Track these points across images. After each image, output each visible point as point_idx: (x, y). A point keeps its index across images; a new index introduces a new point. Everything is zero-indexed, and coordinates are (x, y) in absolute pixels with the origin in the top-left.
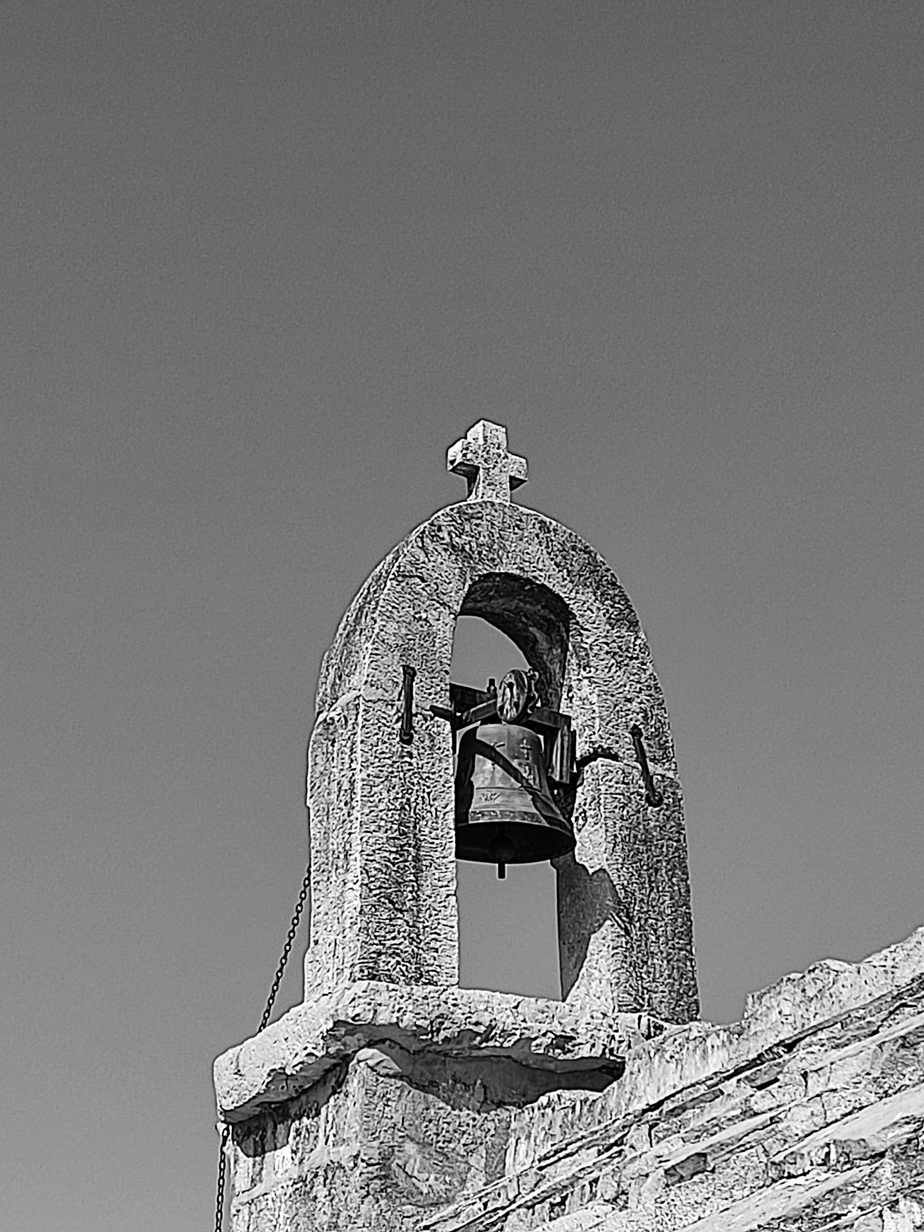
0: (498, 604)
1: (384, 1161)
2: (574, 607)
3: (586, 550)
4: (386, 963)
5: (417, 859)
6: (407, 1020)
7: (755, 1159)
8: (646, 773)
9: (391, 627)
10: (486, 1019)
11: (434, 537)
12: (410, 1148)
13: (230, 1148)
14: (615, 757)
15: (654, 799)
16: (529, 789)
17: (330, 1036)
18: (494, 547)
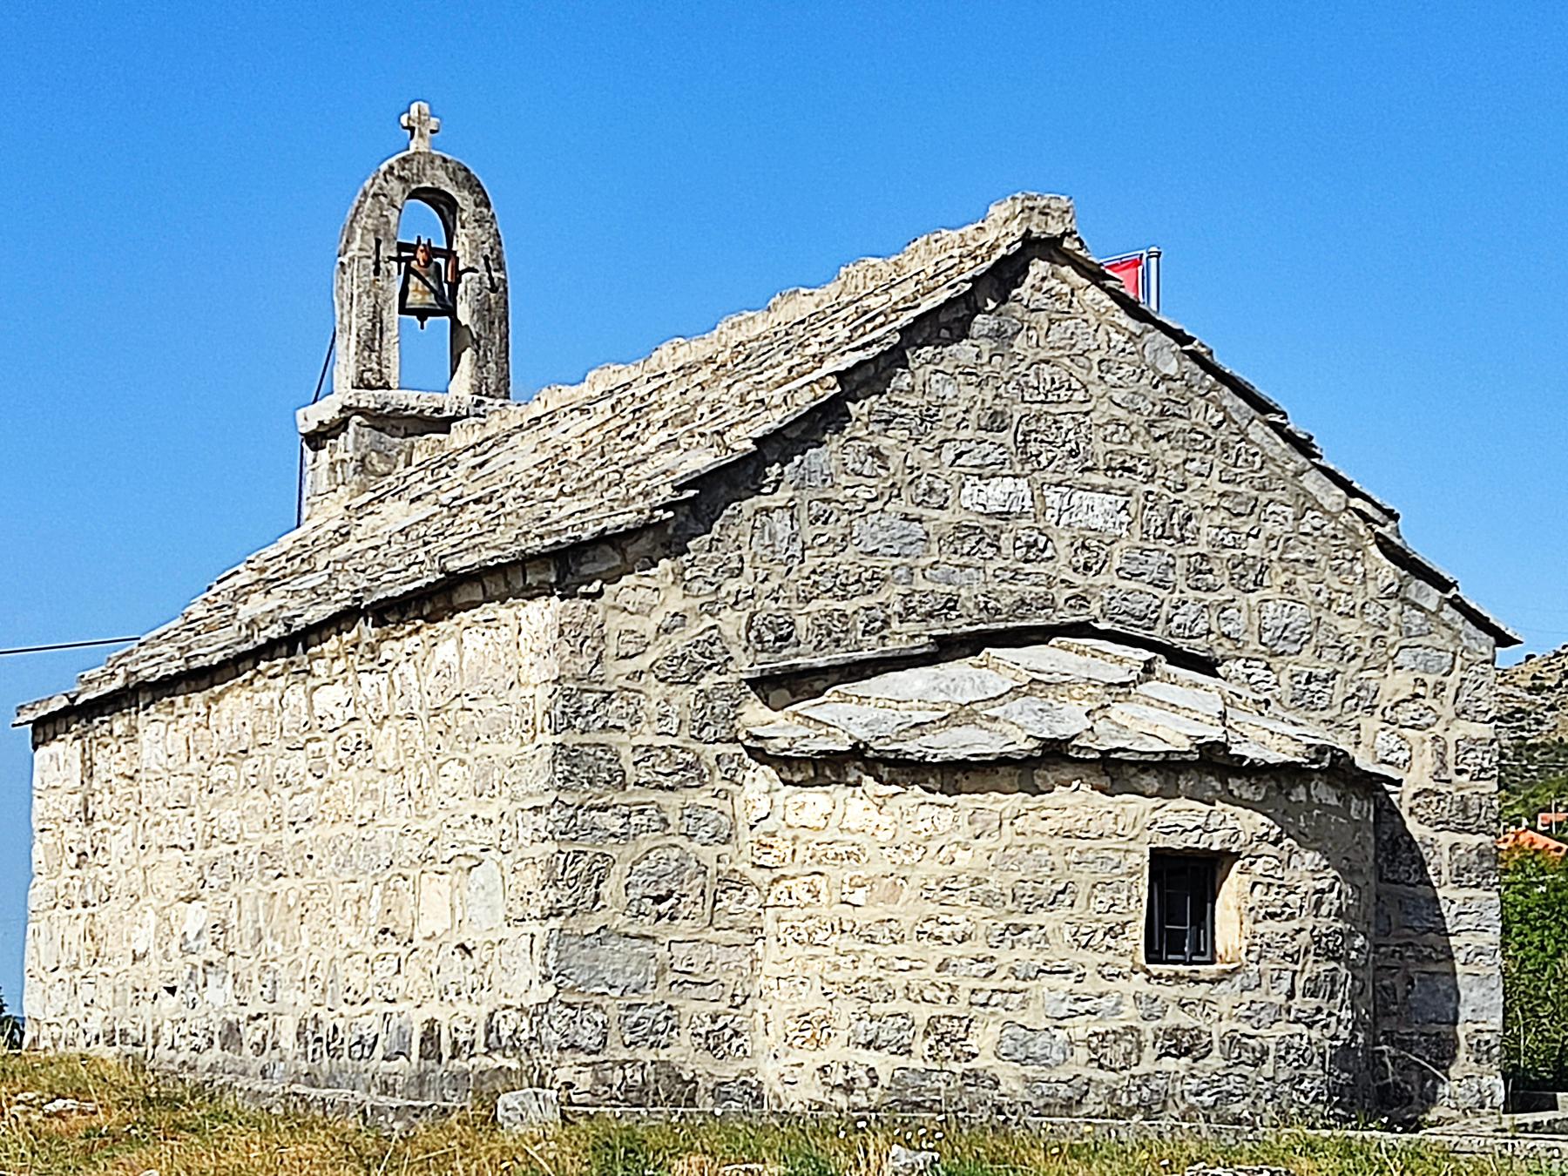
0: (424, 196)
1: (362, 460)
2: (458, 200)
3: (466, 170)
4: (367, 375)
5: (381, 328)
6: (372, 405)
7: (432, 498)
8: (491, 278)
9: (370, 221)
10: (405, 403)
11: (392, 174)
12: (373, 454)
13: (304, 444)
14: (476, 271)
15: (494, 289)
16: (432, 290)
17: (341, 411)
18: (421, 173)
